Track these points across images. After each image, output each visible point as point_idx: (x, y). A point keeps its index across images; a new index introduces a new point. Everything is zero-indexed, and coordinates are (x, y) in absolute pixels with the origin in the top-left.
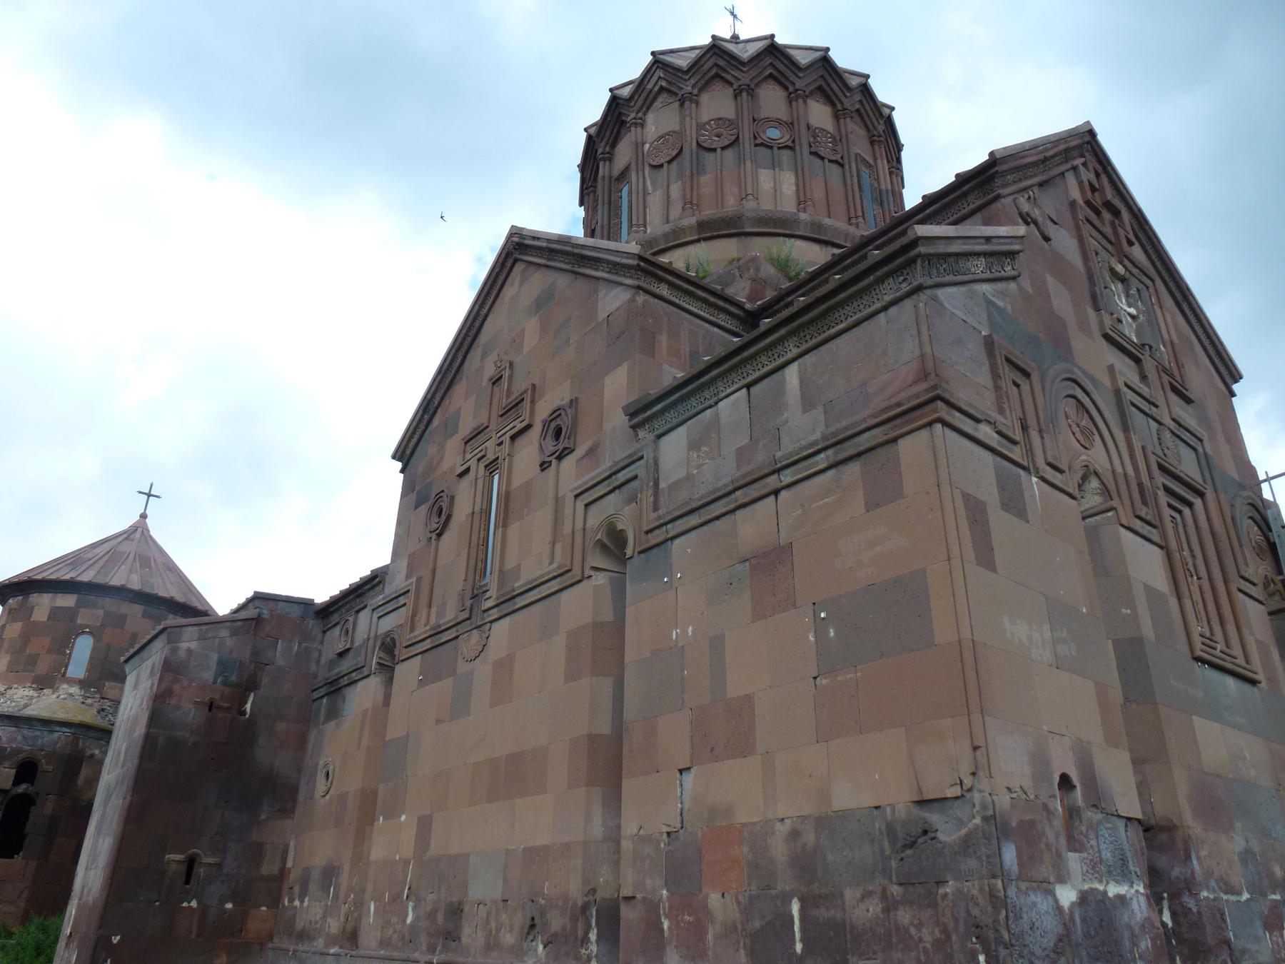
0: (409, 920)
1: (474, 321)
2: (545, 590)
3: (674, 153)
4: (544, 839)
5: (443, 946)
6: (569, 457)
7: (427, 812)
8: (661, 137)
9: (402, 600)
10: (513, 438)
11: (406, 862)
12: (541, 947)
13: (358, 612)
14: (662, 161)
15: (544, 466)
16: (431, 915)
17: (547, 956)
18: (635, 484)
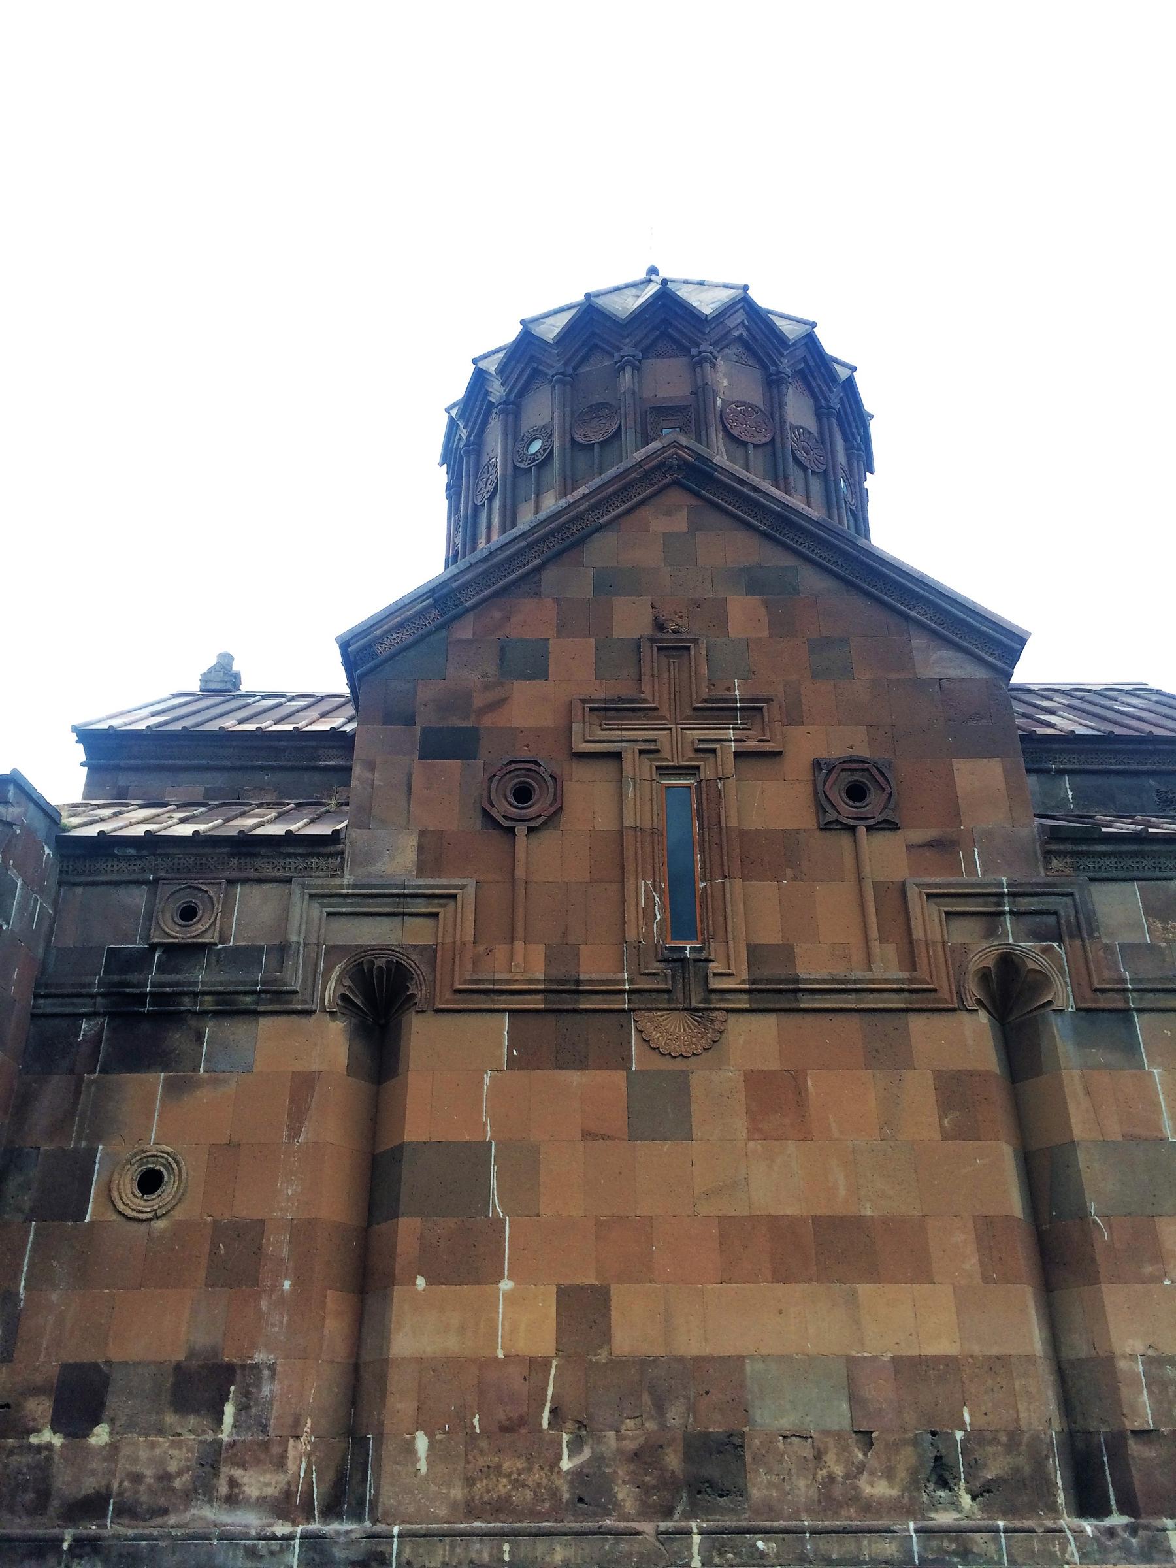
0: (566, 1464)
1: (573, 520)
2: (871, 1002)
3: (764, 440)
4: (944, 1346)
5: (693, 1504)
6: (888, 834)
7: (592, 1281)
8: (742, 404)
9: (421, 907)
10: (738, 755)
11: (537, 1365)
12: (966, 1500)
13: (232, 882)
14: (745, 439)
15: (826, 828)
16: (644, 1457)
17: (985, 1508)
18: (1052, 920)
